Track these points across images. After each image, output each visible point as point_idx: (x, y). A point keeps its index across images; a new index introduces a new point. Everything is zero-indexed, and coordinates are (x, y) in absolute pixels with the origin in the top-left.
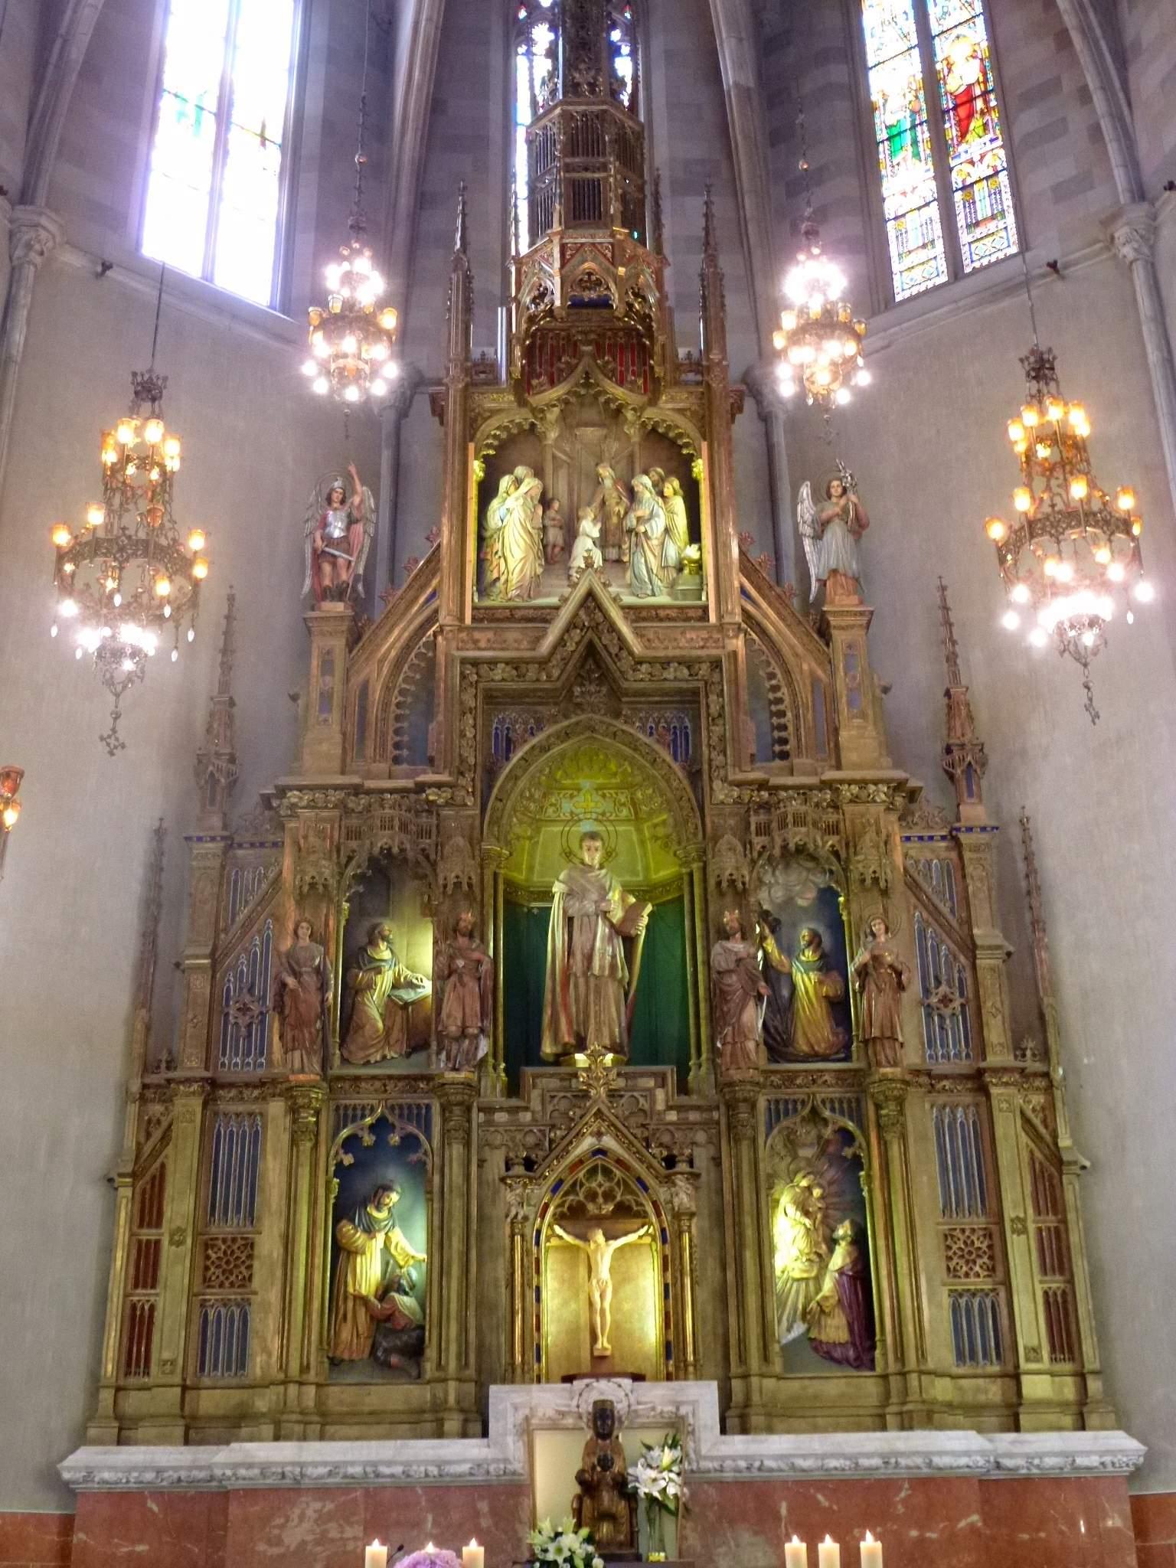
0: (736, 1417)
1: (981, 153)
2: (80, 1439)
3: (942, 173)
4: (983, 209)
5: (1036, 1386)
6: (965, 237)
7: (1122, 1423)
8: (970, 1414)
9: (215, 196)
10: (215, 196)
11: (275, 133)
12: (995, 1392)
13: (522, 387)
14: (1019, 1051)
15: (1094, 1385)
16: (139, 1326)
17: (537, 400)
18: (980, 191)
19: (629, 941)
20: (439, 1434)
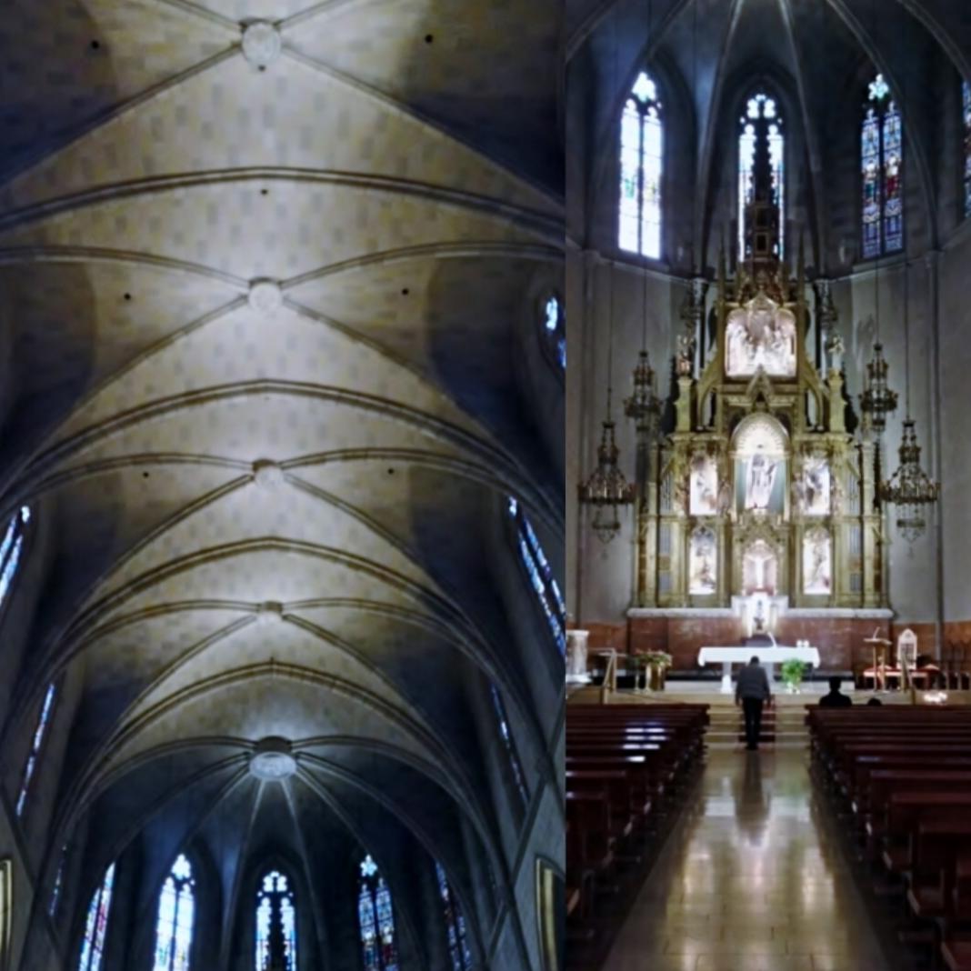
0: (792, 604)
1: (894, 207)
2: (631, 605)
3: (882, 210)
4: (893, 228)
5: (870, 597)
6: (887, 238)
7: (889, 607)
8: (853, 605)
9: (640, 217)
10: (640, 217)
11: (657, 187)
12: (858, 599)
13: (742, 302)
14: (874, 511)
15: (884, 598)
16: (642, 578)
17: (745, 305)
18: (893, 221)
19: (770, 478)
20: (716, 606)
